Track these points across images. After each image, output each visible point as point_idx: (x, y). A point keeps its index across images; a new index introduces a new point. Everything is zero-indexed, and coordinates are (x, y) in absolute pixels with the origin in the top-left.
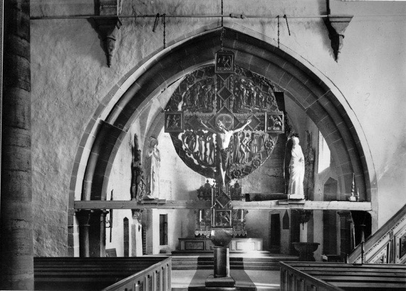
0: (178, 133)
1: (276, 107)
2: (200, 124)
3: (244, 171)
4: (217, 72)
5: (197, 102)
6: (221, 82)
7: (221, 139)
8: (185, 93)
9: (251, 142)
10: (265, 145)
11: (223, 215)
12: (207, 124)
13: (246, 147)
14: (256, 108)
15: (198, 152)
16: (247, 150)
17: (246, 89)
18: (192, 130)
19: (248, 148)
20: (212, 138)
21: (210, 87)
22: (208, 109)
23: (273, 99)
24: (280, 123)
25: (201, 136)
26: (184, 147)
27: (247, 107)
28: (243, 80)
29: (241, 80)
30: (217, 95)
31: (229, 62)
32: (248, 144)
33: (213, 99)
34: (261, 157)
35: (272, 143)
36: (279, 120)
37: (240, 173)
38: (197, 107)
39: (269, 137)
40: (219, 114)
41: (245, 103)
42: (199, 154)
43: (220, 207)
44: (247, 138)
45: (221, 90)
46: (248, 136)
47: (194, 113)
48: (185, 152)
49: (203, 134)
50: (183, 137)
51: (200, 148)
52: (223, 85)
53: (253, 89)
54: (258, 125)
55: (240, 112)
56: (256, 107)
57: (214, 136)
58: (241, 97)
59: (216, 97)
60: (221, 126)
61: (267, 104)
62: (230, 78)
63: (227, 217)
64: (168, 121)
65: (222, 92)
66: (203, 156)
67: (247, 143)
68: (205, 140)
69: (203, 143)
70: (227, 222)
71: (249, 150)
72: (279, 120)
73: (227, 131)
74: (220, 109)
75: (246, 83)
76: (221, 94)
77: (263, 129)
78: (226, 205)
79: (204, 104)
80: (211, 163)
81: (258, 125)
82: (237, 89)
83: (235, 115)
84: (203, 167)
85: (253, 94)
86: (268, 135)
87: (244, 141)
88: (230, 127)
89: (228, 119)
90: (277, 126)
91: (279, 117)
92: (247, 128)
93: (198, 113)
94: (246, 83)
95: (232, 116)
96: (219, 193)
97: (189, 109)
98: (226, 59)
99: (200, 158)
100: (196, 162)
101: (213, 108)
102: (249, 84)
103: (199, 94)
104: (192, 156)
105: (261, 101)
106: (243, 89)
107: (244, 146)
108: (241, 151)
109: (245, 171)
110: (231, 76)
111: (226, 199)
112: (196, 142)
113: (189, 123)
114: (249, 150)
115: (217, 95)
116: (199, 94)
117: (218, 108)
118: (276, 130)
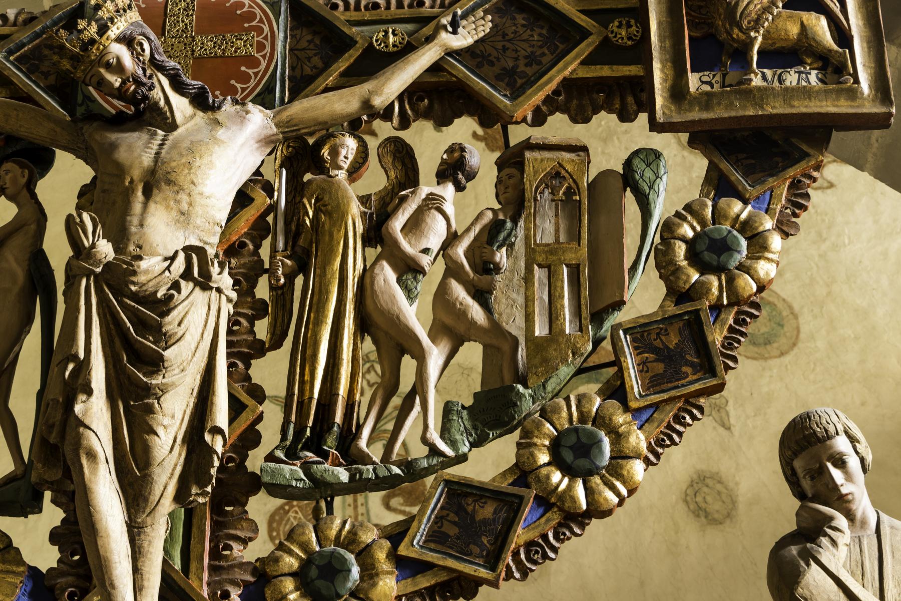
3: (411, 548)
13: (442, 294)
19: (459, 292)
24: (821, 26)
32: (460, 251)
34: (634, 383)
35: (747, 228)
44: (448, 191)
60: (127, 40)
67: (452, 238)
71: (477, 312)
73: (200, 101)
86: (699, 164)
87: (414, 225)
118: (789, 94)
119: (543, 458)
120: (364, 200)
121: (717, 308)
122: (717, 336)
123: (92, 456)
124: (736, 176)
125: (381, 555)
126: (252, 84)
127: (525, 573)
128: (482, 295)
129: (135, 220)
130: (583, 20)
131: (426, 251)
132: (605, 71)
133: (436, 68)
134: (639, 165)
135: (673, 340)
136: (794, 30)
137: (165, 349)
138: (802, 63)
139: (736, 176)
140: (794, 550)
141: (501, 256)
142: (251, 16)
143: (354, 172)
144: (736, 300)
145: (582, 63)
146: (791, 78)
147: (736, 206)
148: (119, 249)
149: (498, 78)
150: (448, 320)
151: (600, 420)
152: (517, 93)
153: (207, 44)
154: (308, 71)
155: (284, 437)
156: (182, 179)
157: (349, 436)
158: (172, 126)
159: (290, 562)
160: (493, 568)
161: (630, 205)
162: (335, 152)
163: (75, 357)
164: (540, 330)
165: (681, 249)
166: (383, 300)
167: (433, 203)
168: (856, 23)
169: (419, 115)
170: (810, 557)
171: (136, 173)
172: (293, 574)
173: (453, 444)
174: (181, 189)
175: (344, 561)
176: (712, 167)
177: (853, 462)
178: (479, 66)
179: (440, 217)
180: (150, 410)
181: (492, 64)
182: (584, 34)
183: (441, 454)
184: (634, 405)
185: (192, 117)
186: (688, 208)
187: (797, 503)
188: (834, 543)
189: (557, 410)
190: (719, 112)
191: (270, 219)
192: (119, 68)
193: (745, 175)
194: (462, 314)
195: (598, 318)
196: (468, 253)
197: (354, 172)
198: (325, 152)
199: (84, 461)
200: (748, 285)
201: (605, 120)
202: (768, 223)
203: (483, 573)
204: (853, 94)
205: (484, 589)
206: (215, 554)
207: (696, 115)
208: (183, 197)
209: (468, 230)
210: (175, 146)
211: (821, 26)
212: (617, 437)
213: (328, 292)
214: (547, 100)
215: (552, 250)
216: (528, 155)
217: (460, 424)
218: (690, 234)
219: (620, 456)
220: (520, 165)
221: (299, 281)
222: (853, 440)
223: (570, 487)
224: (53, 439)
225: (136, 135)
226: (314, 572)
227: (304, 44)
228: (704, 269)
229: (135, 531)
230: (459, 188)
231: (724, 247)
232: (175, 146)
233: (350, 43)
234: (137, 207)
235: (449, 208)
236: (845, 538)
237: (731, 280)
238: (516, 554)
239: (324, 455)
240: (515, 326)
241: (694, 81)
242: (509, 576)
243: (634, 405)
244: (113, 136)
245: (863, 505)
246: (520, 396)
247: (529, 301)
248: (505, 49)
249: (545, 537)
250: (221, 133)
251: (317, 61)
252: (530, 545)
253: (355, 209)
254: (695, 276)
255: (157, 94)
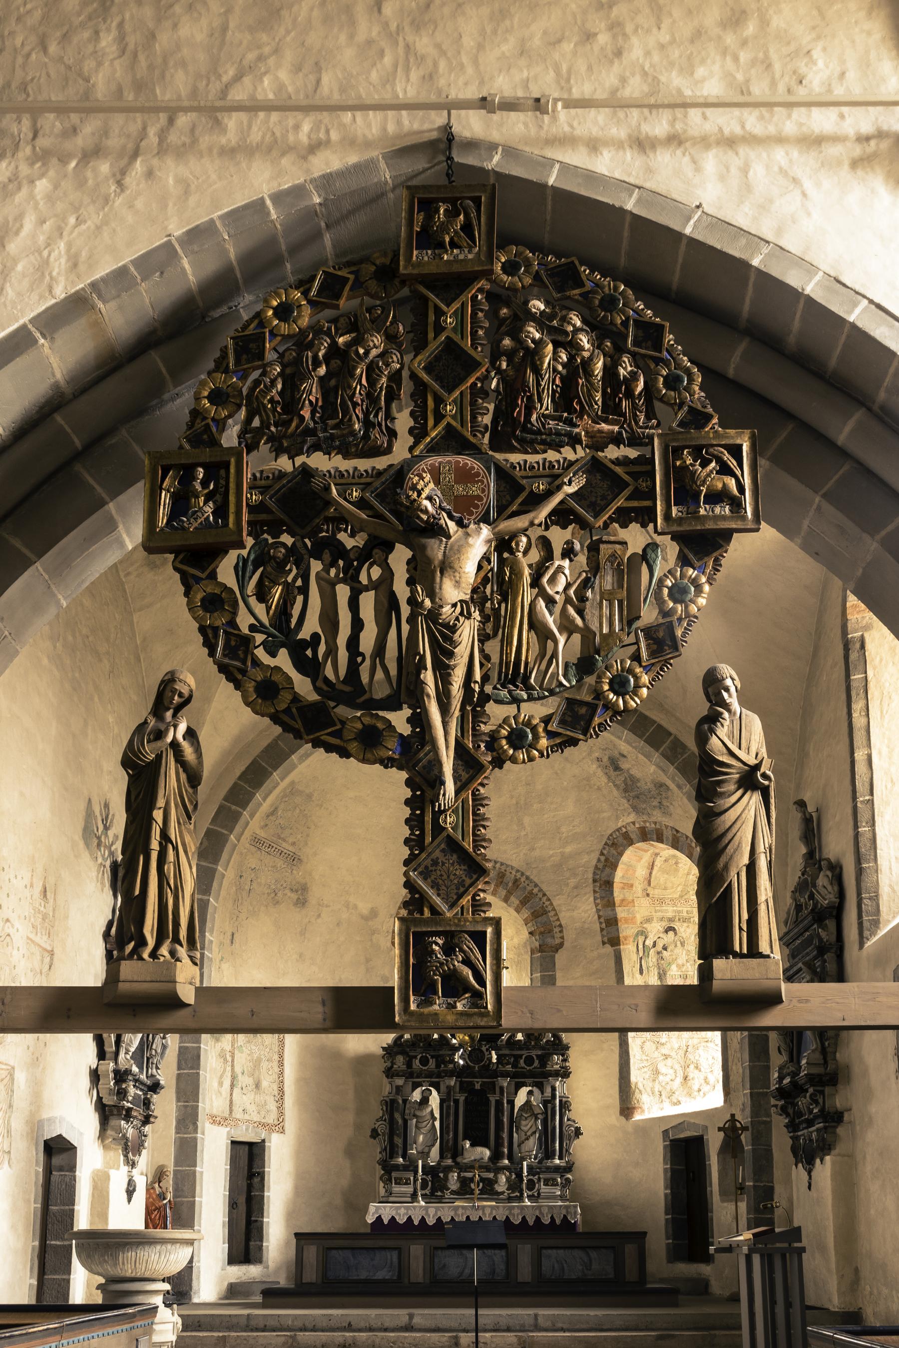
0: (219, 551)
1: (709, 417)
2: (329, 502)
3: (553, 726)
4: (410, 270)
5: (313, 413)
6: (432, 317)
7: (429, 561)
8: (255, 375)
9: (586, 584)
10: (659, 601)
11: (448, 950)
12: (362, 504)
13: (564, 610)
14: (605, 427)
15: (315, 637)
16: (567, 627)
17: (557, 345)
18: (287, 539)
19: (571, 611)
20: (388, 574)
21: (377, 341)
22: (366, 437)
23: (691, 381)
24: (732, 483)
25: (333, 564)
26: (244, 621)
27: (559, 419)
28: (538, 305)
29: (526, 303)
30: (413, 376)
31: (467, 228)
32: (571, 592)
33: (392, 396)
34: (644, 654)
35: (695, 582)
36: (725, 470)
37: (536, 737)
38: (311, 432)
39: (684, 561)
40: (420, 458)
41: (547, 401)
42: (322, 649)
43: (434, 911)
44: (566, 563)
45: (434, 345)
46: (569, 553)
47: (299, 460)
48: (246, 642)
49: (339, 551)
50: (241, 571)
51: (330, 619)
52: (439, 329)
53: (584, 340)
54: (620, 502)
55: (526, 446)
56: (606, 421)
57: (400, 557)
58: (531, 378)
59: (407, 386)
60: (430, 498)
61: (657, 405)
62: (475, 297)
63: (467, 962)
64: (165, 497)
65: (437, 358)
66: (343, 655)
67: (568, 586)
68: (351, 578)
69: (343, 592)
70: (467, 988)
71: (579, 621)
72: (725, 470)
73: (460, 523)
74: (425, 434)
75: (551, 317)
76: (428, 369)
77: (646, 517)
78: (466, 900)
79: (346, 412)
80: (381, 692)
81: (620, 502)
82: (507, 342)
83: (499, 456)
84: (343, 711)
85: (587, 365)
87: (553, 580)
88: (479, 512)
89: (465, 476)
90: (715, 497)
91: (727, 457)
92: (561, 517)
93: (319, 461)
94: (551, 317)
95: (487, 462)
96: (428, 839)
97: (271, 439)
98: (452, 214)
99: (329, 672)
100: (303, 685)
101: (392, 434)
102: (565, 319)
103: (322, 370)
104: (283, 660)
105: (629, 394)
106: (539, 343)
107: (550, 602)
108: (536, 625)
109: (562, 722)
110: (480, 290)
111: (459, 871)
112: (304, 591)
113: (271, 504)
114: (579, 621)
115: (413, 376)
116: (322, 370)
117: (418, 433)
118: (717, 518)
119: (606, 687)
120: (530, 566)
121: (680, 619)
122: (679, 633)
123: (428, 696)
124: (691, 556)
125: (541, 730)
126: (480, 510)
127: (597, 736)
128: (580, 612)
129: (438, 587)
130: (626, 478)
131: (557, 593)
132: (635, 504)
133: (562, 502)
134: (649, 551)
135: (661, 634)
136: (720, 485)
137: (455, 648)
138: (722, 501)
139: (691, 556)
140: (706, 727)
141: (589, 594)
142: (478, 474)
143: (525, 553)
144: (688, 615)
145: (626, 499)
146: (718, 510)
147: (691, 571)
148: (433, 601)
149: (589, 506)
150: (567, 624)
151: (630, 671)
152: (596, 516)
153: (460, 489)
154: (504, 502)
155: (499, 679)
156: (456, 566)
157: (526, 677)
158: (448, 537)
159: (504, 732)
160: (585, 735)
161: (644, 569)
162: (517, 545)
163: (419, 653)
164: (605, 630)
165: (666, 591)
166: (539, 616)
167: (560, 569)
168: (747, 482)
169: (553, 523)
170: (712, 731)
171: (436, 563)
172: (505, 738)
173: (569, 681)
174: (455, 571)
175: (526, 732)
176: (681, 551)
177: (733, 689)
178: (580, 500)
179: (563, 576)
180: (450, 675)
181: (585, 499)
182: (627, 485)
183: (565, 686)
184: (644, 664)
185: (457, 531)
186: (669, 572)
187: (709, 704)
188: (722, 725)
189: (612, 666)
190: (685, 528)
191: (490, 575)
192: (426, 511)
193: (695, 555)
194: (573, 621)
195: (630, 623)
196: (575, 592)
197: (525, 553)
198: (513, 544)
199: (426, 699)
200: (693, 609)
201: (634, 527)
202: (703, 579)
203: (581, 737)
204: (744, 518)
205: (581, 742)
206: (474, 729)
207: (675, 528)
208: (457, 574)
209: (575, 582)
210: (451, 549)
211: (732, 483)
212: (637, 678)
213: (516, 612)
214: (610, 517)
215: (611, 593)
216: (602, 546)
217: (572, 671)
218: (670, 584)
219: (638, 686)
220: (598, 551)
221: (503, 605)
222: (733, 679)
223: (617, 700)
224: (412, 688)
225: (433, 540)
226: (514, 737)
227: (502, 489)
228: (676, 601)
229: (445, 724)
230: (571, 560)
231: (684, 591)
232: (451, 549)
233: (522, 488)
234: (438, 580)
235: (567, 572)
236: (727, 723)
237: (686, 607)
238: (594, 728)
239: (517, 687)
240: (594, 627)
241: (674, 511)
242: (591, 736)
243: (644, 664)
244: (424, 541)
245: (736, 706)
246: (597, 660)
247: (601, 617)
248: (591, 492)
249: (606, 721)
250: (471, 540)
251: (508, 497)
252: (600, 725)
253: (527, 572)
254: (671, 604)
255: (442, 522)
